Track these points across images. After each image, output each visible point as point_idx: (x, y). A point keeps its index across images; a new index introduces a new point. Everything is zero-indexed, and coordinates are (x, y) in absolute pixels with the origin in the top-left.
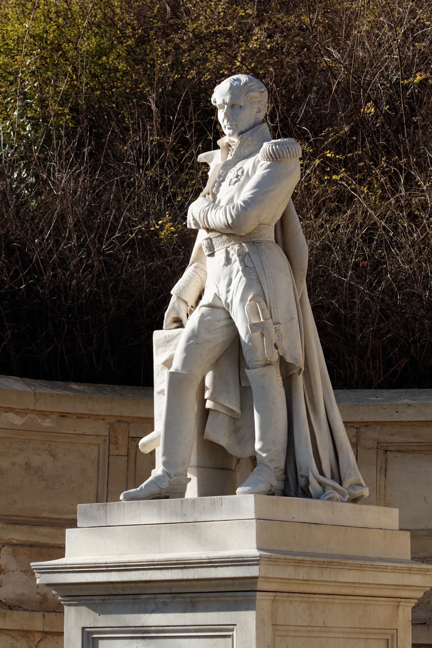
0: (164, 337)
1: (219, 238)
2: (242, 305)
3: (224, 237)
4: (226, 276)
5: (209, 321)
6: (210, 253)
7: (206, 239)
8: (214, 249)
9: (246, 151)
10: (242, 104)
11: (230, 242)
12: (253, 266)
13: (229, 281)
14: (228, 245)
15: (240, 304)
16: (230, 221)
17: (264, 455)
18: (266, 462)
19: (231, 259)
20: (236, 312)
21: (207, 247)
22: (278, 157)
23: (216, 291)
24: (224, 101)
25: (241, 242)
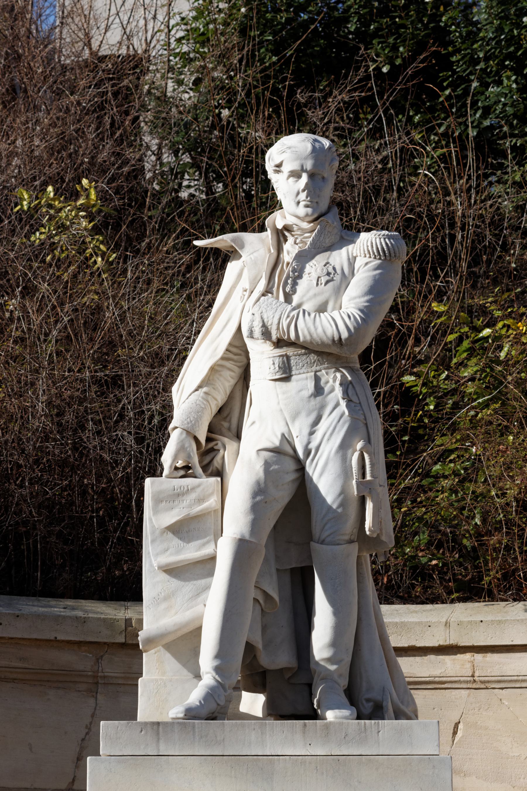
1: (305, 357)
2: (340, 454)
3: (313, 357)
5: (277, 471)
6: (283, 376)
7: (280, 356)
9: (327, 241)
10: (325, 176)
11: (321, 364)
12: (358, 402)
14: (318, 368)
15: (337, 452)
16: (345, 335)
18: (336, 677)
19: (323, 389)
21: (279, 367)
22: (393, 255)
23: (285, 430)
24: (302, 166)
25: (338, 366)
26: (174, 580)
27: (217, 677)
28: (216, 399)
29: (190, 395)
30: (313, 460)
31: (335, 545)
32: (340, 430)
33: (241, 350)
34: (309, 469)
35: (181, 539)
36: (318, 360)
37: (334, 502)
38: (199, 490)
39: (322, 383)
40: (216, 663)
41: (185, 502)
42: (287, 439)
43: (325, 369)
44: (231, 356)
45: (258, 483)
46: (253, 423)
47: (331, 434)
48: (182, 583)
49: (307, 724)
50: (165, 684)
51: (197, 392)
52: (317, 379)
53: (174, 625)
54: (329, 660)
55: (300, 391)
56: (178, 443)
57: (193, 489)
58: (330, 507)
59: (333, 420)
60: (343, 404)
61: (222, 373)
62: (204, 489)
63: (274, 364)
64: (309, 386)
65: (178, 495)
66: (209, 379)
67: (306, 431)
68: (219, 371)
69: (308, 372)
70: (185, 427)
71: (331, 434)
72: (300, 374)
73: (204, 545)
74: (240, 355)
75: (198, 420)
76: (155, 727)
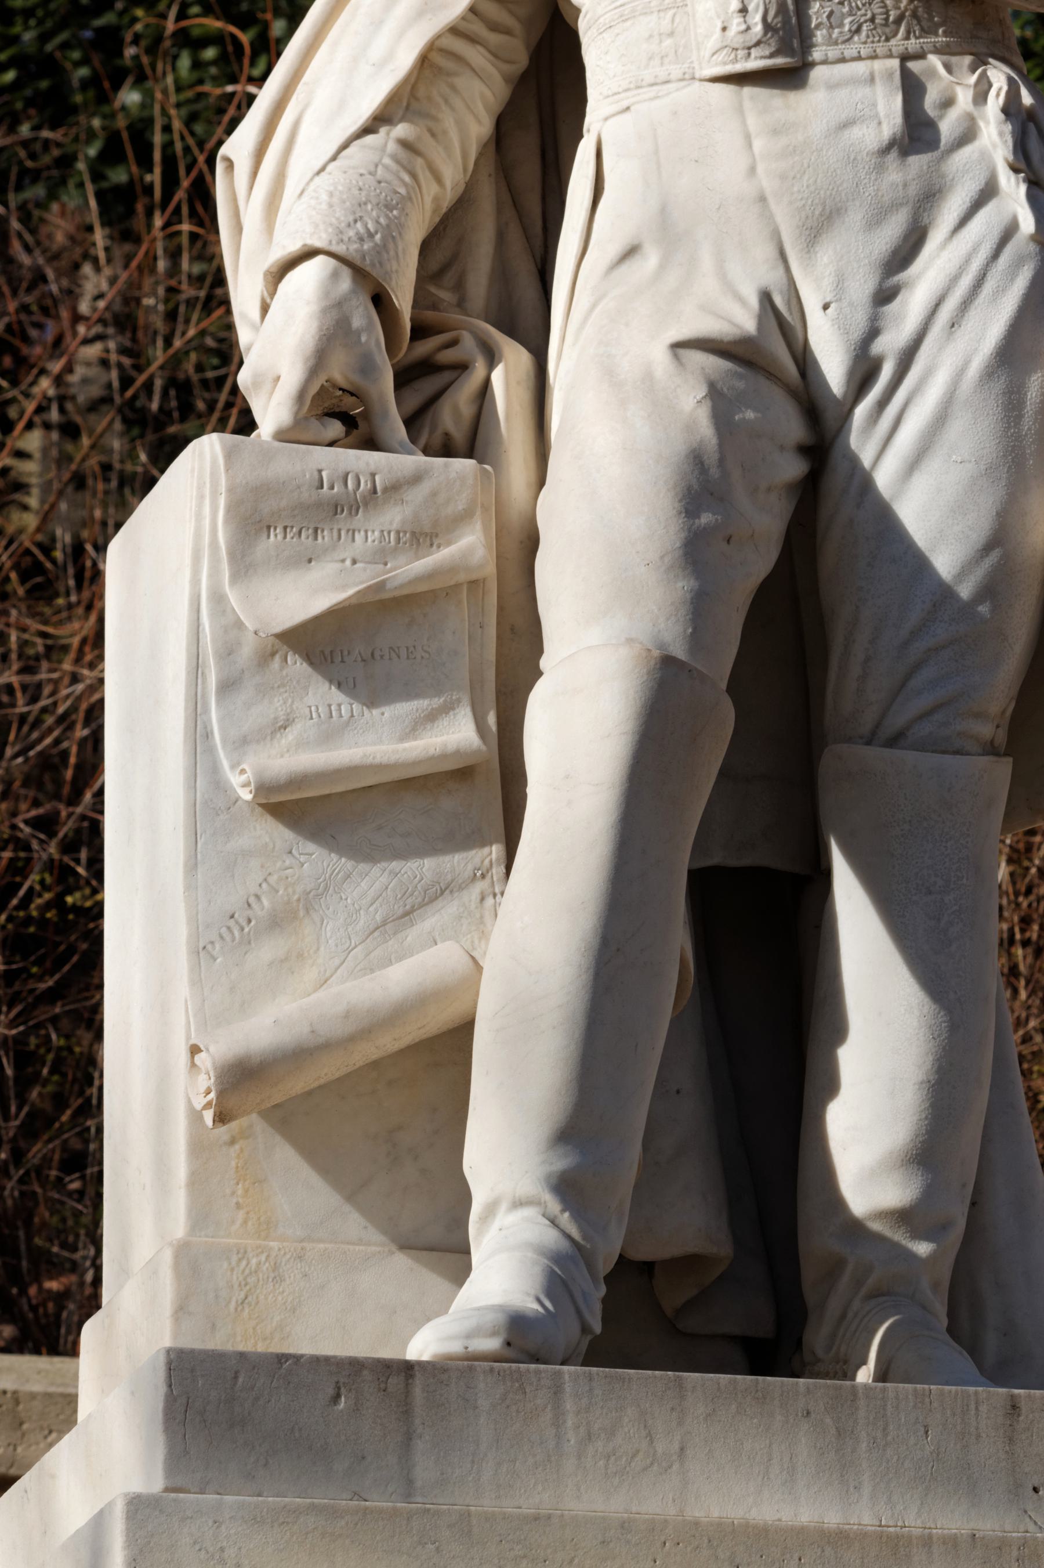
0: (309, 476)
2: (999, 385)
4: (895, 206)
6: (780, 61)
8: (806, 43)
11: (925, 32)
13: (906, 237)
15: (990, 373)
17: (923, 1248)
21: (767, 26)
23: (773, 278)
26: (311, 847)
27: (565, 1218)
28: (438, 179)
29: (345, 146)
30: (882, 404)
31: (944, 752)
32: (1000, 291)
33: (511, 13)
34: (862, 441)
35: (339, 686)
36: (915, 15)
38: (416, 496)
40: (560, 1163)
41: (359, 537)
42: (782, 318)
43: (937, 51)
44: (478, 28)
45: (696, 458)
46: (631, 252)
47: (966, 304)
48: (345, 864)
49: (1024, 1408)
50: (275, 1268)
51: (369, 139)
52: (912, 89)
53: (347, 1015)
54: (902, 1217)
55: (846, 125)
56: (324, 311)
57: (395, 488)
59: (975, 249)
61: (460, 82)
62: (434, 494)
63: (744, 11)
64: (881, 109)
65: (332, 510)
66: (413, 95)
67: (862, 286)
68: (449, 74)
69: (874, 57)
70: (349, 249)
71: (966, 304)
72: (843, 60)
73: (431, 717)
74: (507, 32)
75: (392, 232)
76: (395, 1383)
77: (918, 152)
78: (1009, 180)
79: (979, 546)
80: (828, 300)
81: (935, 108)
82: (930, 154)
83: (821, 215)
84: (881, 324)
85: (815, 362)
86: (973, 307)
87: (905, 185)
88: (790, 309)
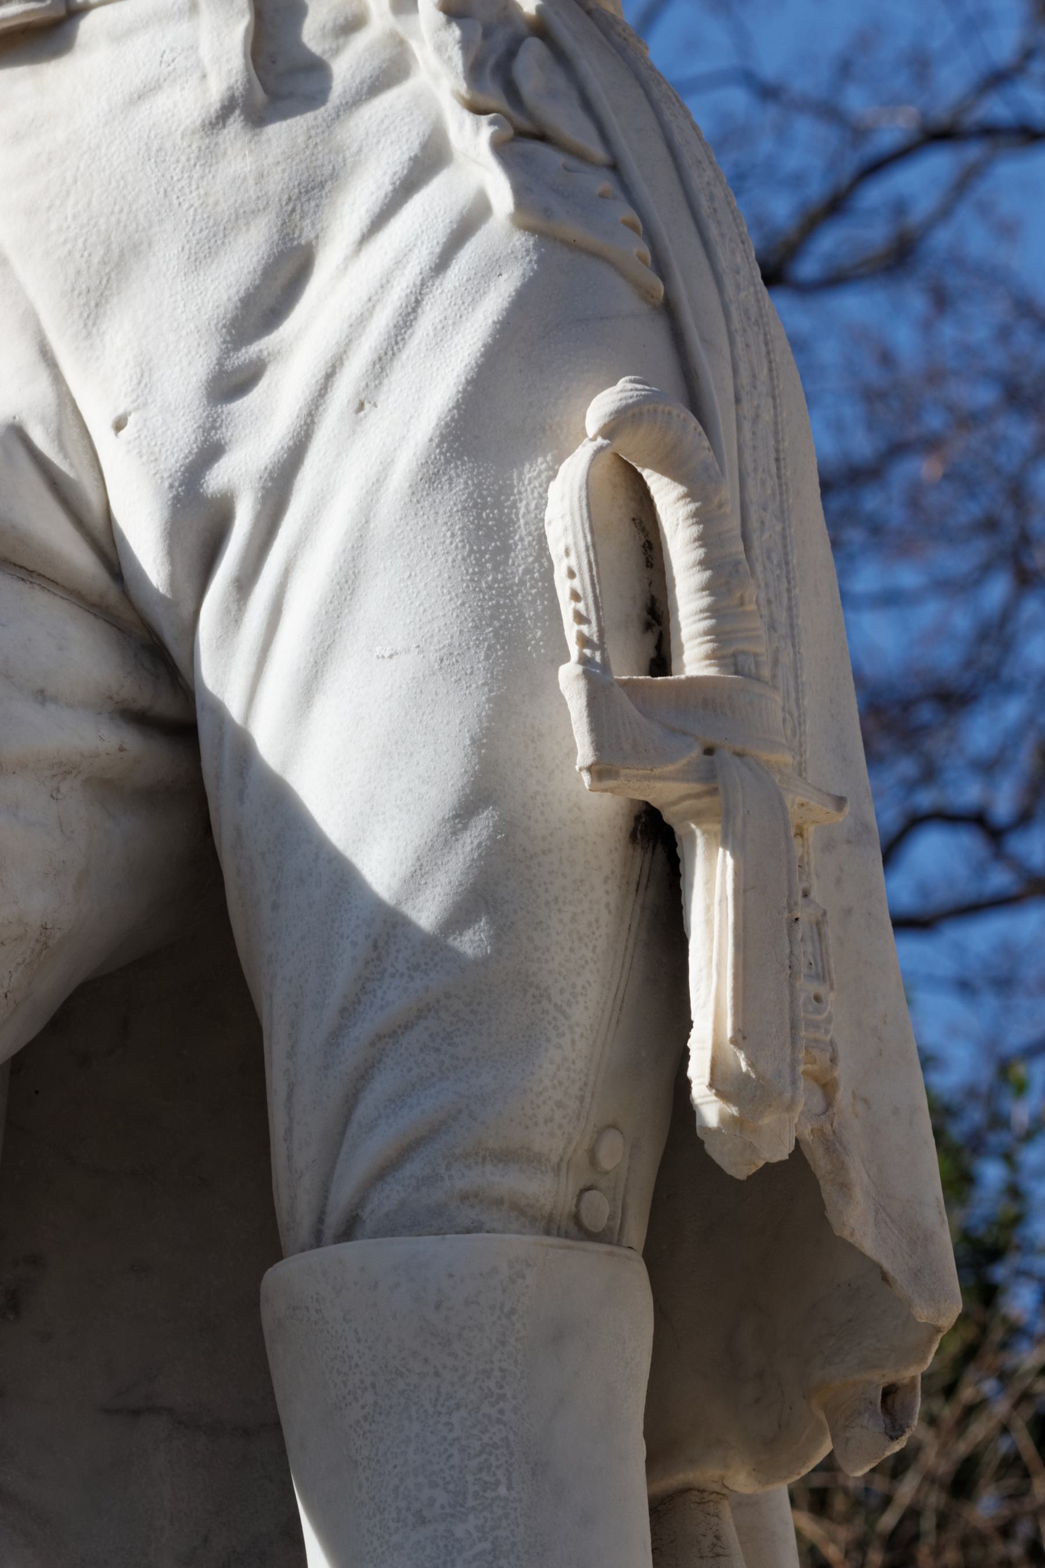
2: (455, 493)
4: (241, 217)
13: (269, 271)
15: (431, 477)
19: (316, 70)
20: (347, 584)
37: (417, 877)
39: (312, 34)
47: (382, 364)
58: (390, 923)
59: (399, 263)
60: (472, 140)
64: (205, 52)
71: (382, 364)
77: (284, 116)
78: (461, 126)
79: (446, 811)
80: (121, 411)
81: (324, 36)
82: (310, 116)
83: (104, 262)
84: (225, 434)
85: (123, 538)
86: (397, 364)
87: (261, 176)
88: (62, 448)
